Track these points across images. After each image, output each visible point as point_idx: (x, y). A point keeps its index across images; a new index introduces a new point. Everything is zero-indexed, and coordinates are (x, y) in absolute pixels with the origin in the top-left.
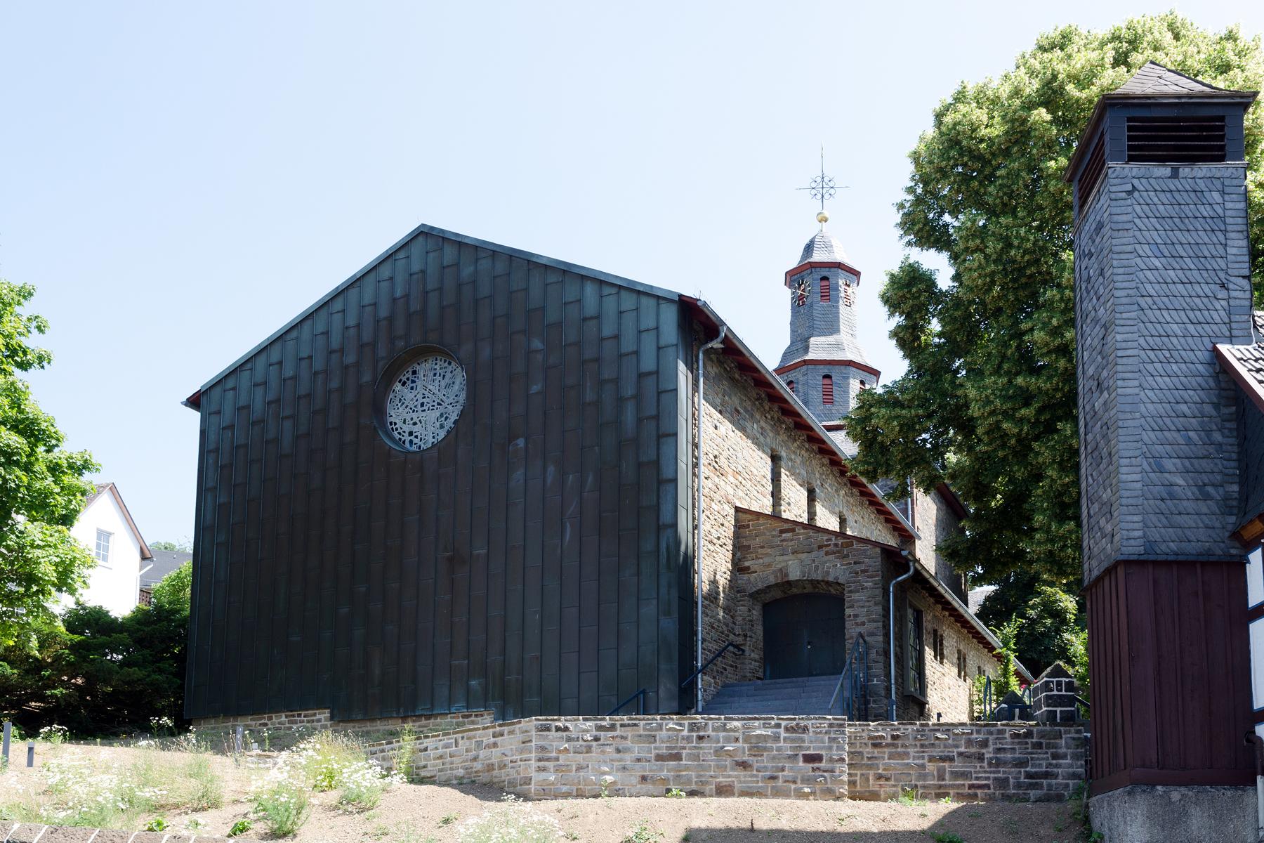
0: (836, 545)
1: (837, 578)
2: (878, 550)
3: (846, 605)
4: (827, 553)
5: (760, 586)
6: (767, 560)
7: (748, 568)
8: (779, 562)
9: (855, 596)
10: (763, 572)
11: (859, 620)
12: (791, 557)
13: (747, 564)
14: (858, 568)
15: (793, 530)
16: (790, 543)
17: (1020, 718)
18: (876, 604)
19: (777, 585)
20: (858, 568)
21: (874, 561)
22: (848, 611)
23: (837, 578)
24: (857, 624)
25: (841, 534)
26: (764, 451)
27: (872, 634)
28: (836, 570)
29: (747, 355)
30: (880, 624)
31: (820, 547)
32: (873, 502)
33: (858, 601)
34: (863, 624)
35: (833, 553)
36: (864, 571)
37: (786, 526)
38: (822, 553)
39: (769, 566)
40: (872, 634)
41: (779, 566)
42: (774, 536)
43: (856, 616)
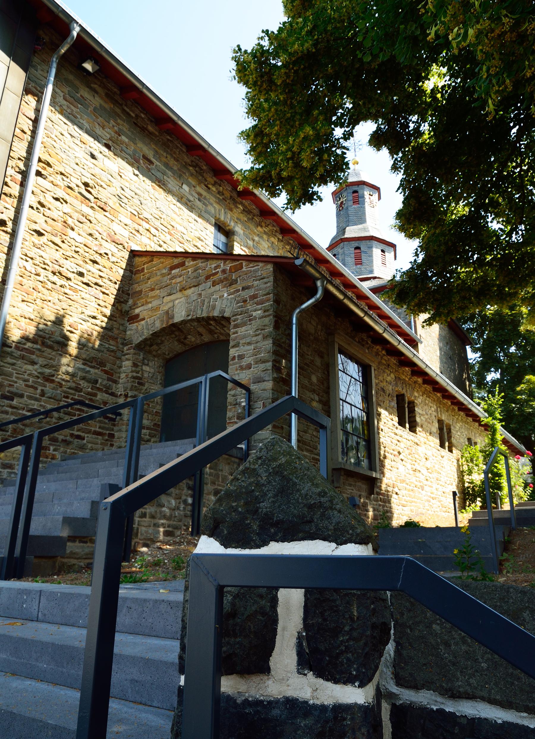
0: (224, 271)
1: (223, 311)
2: (270, 267)
3: (232, 344)
4: (214, 284)
5: (146, 334)
6: (155, 303)
7: (138, 316)
8: (166, 304)
9: (242, 331)
10: (150, 316)
11: (244, 363)
12: (179, 295)
13: (137, 311)
14: (246, 294)
15: (183, 264)
16: (179, 280)
17: (315, 659)
18: (265, 338)
19: (163, 330)
20: (246, 294)
21: (263, 280)
22: (232, 352)
23: (223, 311)
24: (242, 368)
25: (227, 255)
26: (207, 221)
27: (259, 380)
28: (222, 301)
29: (214, 154)
30: (269, 365)
31: (208, 278)
32: (267, 213)
33: (244, 337)
34: (249, 367)
35: (221, 281)
36: (254, 297)
37: (176, 261)
38: (209, 283)
39: (157, 308)
40: (259, 380)
41: (166, 308)
42: (163, 275)
43: (241, 357)
